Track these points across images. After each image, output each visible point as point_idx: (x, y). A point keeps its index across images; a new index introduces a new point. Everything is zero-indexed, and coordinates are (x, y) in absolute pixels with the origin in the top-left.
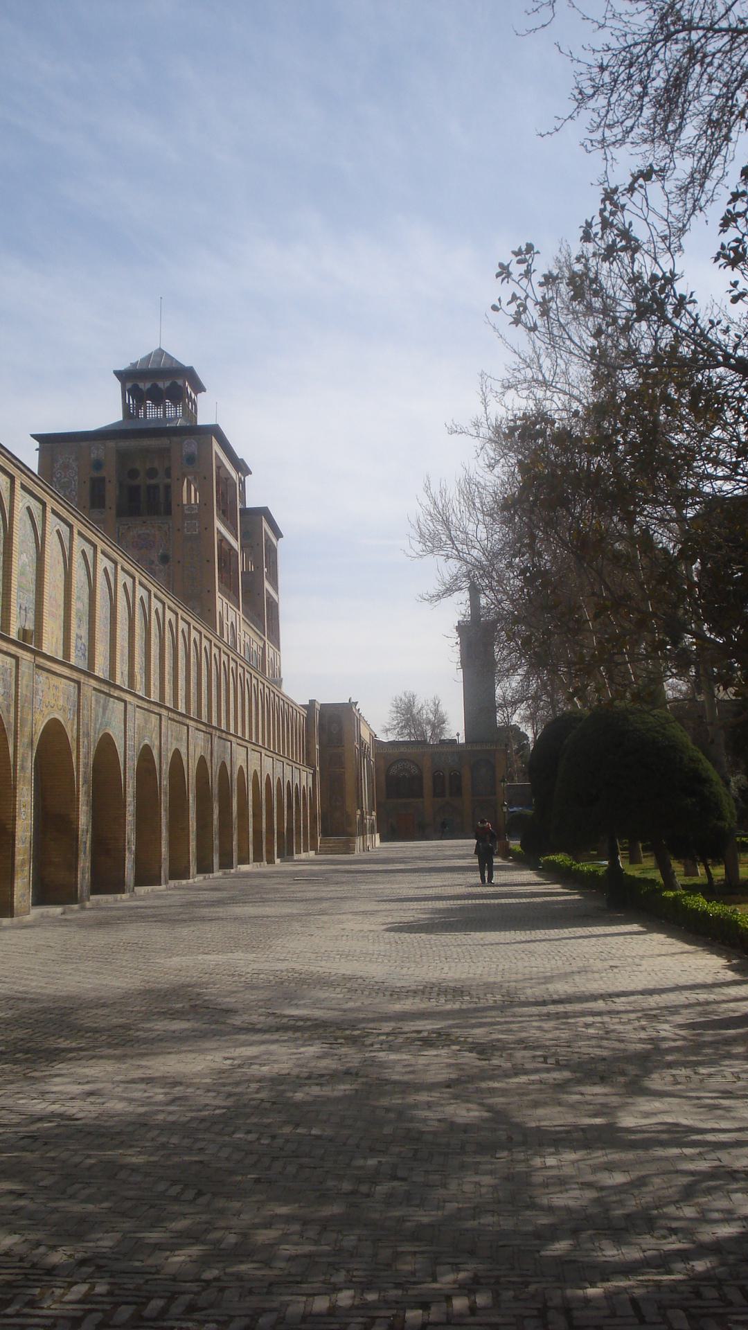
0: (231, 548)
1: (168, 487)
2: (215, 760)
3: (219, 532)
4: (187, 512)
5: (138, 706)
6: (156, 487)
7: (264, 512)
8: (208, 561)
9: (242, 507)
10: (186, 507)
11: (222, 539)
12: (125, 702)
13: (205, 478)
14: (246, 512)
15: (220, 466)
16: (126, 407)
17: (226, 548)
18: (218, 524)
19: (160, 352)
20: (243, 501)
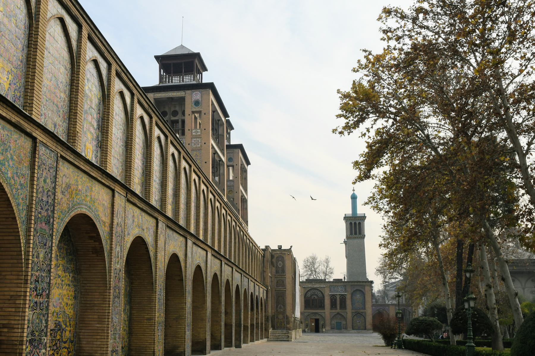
0: (221, 160)
1: (183, 122)
2: (189, 260)
3: (213, 147)
4: (194, 134)
5: (62, 157)
6: (177, 122)
7: (240, 147)
8: (206, 162)
9: (228, 144)
10: (194, 131)
11: (215, 153)
12: (34, 139)
13: (205, 114)
14: (230, 147)
15: (214, 111)
16: (161, 77)
17: (218, 159)
18: (212, 142)
19: (182, 47)
20: (229, 139)
